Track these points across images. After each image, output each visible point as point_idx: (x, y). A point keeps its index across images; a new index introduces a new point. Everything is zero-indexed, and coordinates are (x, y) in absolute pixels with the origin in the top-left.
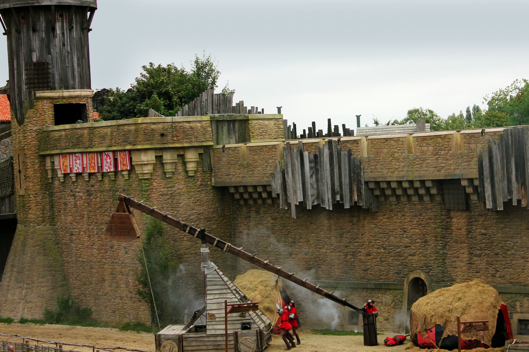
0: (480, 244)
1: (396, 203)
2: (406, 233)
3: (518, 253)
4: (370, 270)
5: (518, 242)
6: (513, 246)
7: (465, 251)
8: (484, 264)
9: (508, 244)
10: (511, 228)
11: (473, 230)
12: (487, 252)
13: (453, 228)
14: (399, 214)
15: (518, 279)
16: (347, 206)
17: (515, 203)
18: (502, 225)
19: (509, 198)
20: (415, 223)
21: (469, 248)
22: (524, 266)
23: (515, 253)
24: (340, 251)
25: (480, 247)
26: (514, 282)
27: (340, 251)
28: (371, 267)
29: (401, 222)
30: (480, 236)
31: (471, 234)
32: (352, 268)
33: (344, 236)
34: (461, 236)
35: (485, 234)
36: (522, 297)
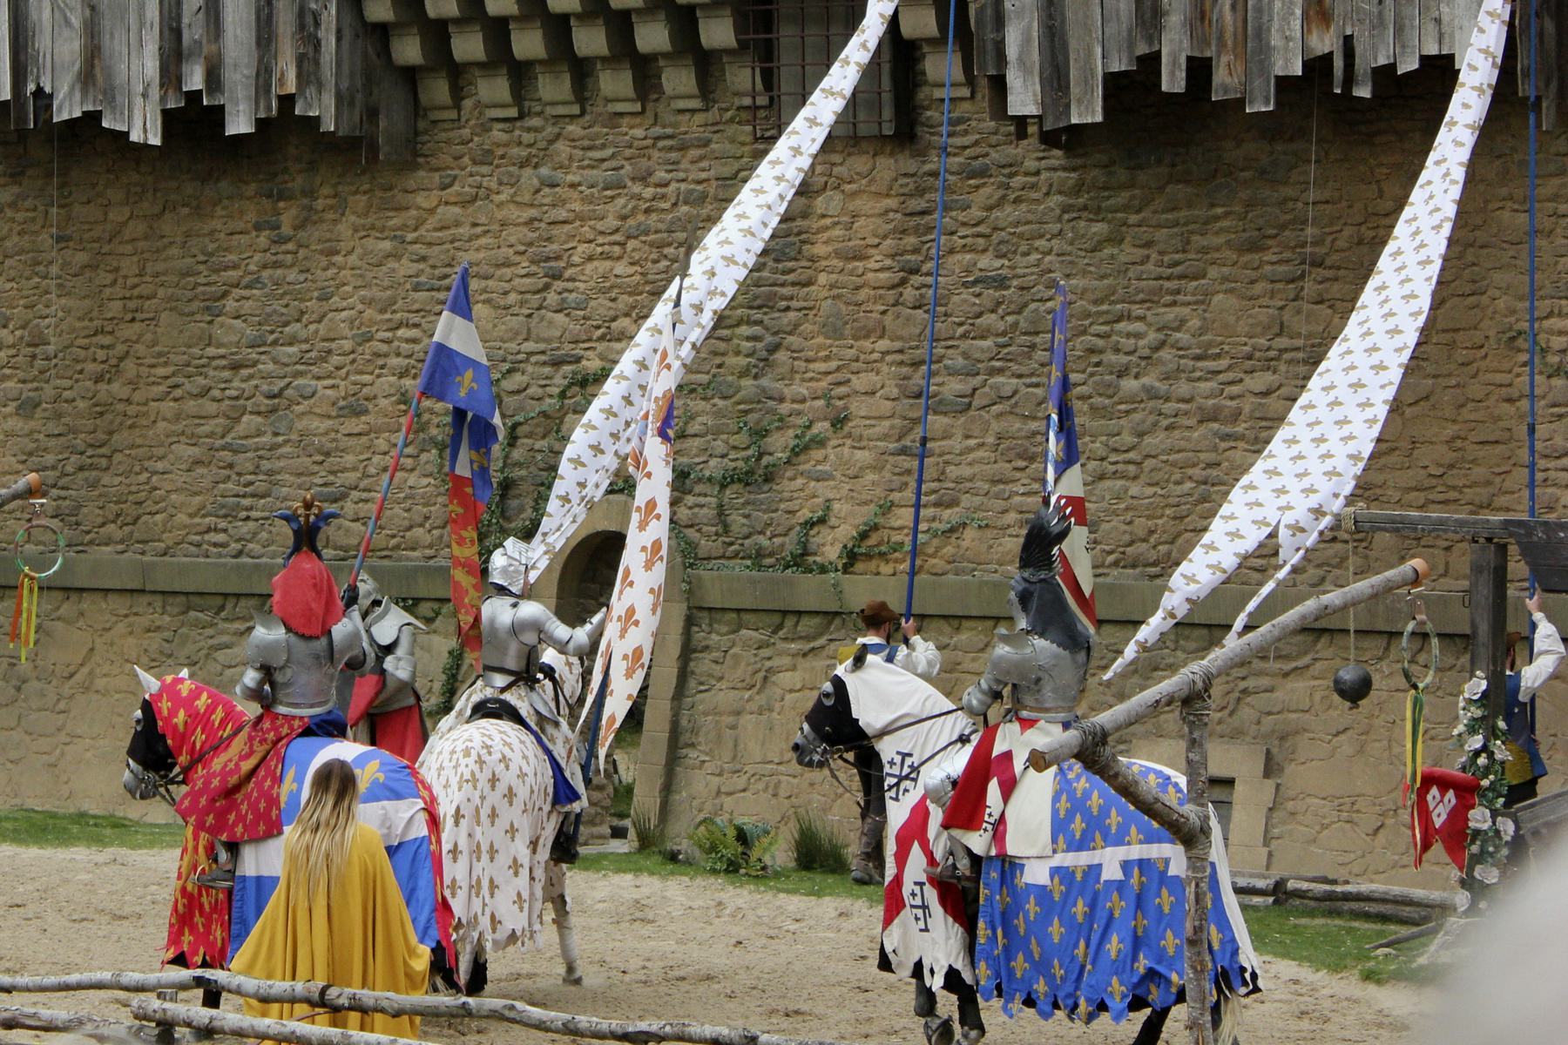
0: (964, 336)
1: (513, 112)
2: (559, 285)
3: (1183, 388)
4: (355, 494)
5: (1183, 322)
6: (1161, 345)
7: (886, 378)
8: (980, 454)
9: (1128, 335)
10: (1148, 244)
11: (928, 258)
12: (1006, 383)
13: (820, 249)
14: (528, 171)
15: (1172, 542)
16: (239, 124)
17: (1173, 80)
18: (1099, 228)
19: (1142, 49)
20: (611, 222)
21: (902, 363)
22: (1210, 465)
23: (1162, 387)
24: (204, 392)
25: (966, 355)
26: (1152, 555)
27: (204, 392)
28: (366, 476)
29: (532, 220)
30: (966, 294)
31: (916, 280)
32: (260, 487)
33: (230, 304)
34: (863, 294)
35: (1001, 283)
36: (1192, 645)
